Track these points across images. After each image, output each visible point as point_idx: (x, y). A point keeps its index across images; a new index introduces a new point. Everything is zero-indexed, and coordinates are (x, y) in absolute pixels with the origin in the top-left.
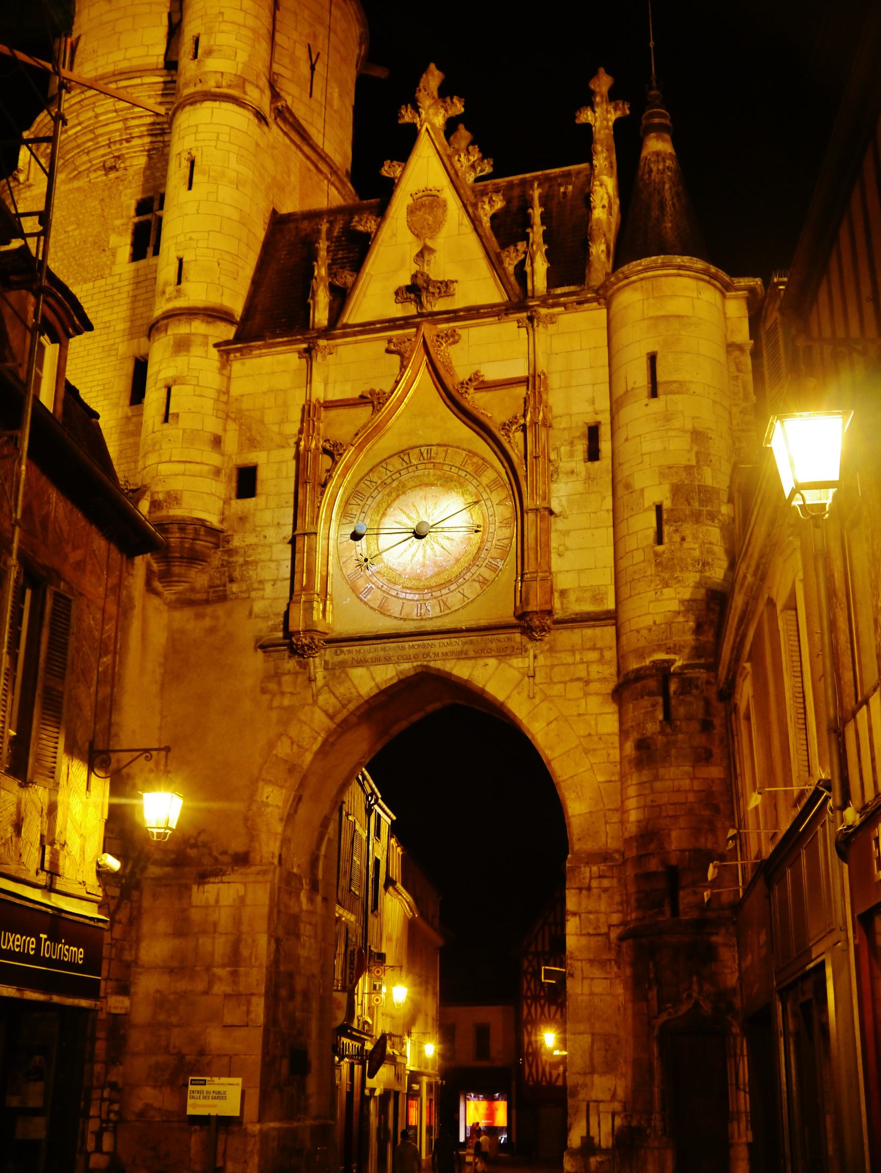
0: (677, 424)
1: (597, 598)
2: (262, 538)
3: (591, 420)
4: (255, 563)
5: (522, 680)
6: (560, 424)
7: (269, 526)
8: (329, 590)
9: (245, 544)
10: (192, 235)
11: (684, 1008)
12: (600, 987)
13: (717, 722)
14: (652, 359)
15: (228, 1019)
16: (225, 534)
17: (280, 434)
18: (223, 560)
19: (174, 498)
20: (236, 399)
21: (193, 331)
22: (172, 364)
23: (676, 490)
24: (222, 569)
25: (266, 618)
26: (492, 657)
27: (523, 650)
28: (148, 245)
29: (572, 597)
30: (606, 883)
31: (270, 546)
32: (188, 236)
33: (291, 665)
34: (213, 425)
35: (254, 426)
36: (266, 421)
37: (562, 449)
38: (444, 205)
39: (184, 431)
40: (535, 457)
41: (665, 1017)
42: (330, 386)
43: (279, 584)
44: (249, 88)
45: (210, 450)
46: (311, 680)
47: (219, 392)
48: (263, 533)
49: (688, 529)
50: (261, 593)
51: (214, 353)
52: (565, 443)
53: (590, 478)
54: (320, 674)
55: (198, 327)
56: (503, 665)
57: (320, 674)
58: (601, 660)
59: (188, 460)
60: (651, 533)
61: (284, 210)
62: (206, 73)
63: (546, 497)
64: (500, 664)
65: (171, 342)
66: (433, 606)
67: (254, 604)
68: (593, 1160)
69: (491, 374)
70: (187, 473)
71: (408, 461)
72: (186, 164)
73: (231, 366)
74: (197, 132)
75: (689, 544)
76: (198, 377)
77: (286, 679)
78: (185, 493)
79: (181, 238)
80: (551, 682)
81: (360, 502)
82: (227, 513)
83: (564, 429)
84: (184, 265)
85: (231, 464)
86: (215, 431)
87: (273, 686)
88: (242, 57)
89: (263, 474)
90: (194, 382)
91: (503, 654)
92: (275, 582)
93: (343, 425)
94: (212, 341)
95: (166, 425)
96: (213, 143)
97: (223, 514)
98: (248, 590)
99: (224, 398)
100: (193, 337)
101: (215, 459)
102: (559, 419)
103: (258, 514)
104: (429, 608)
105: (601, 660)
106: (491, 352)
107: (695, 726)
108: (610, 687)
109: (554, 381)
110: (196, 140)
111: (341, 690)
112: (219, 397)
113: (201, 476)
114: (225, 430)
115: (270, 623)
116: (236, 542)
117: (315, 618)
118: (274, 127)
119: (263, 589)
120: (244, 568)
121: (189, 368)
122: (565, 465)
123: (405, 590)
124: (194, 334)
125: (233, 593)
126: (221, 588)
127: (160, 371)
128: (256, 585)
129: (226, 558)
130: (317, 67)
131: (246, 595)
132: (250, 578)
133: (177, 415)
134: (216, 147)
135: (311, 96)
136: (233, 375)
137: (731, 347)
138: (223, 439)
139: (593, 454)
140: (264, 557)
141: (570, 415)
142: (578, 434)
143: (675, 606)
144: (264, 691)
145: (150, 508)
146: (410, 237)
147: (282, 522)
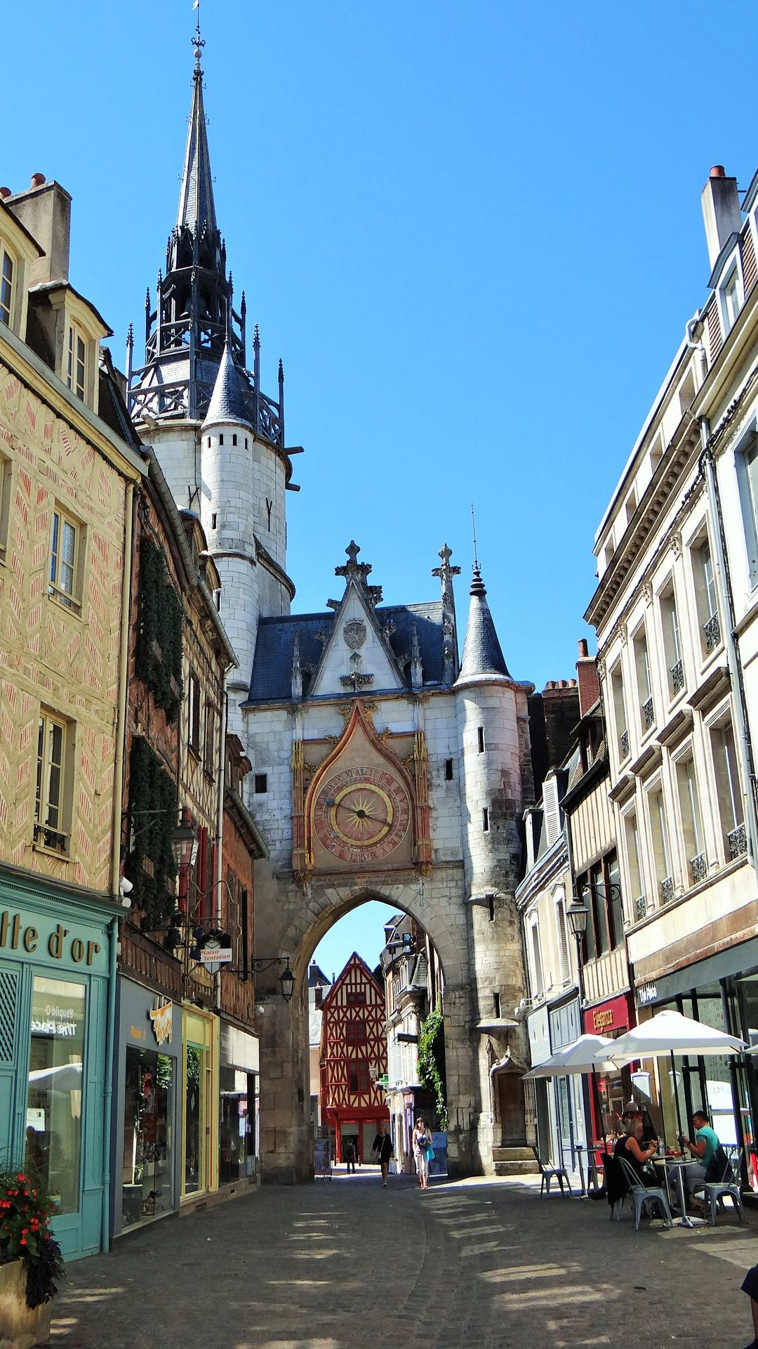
3: (448, 758)
11: (503, 1061)
14: (480, 730)
15: (272, 1075)
23: (495, 803)
25: (278, 861)
29: (441, 853)
30: (463, 1000)
33: (293, 887)
41: (495, 1066)
46: (304, 895)
53: (448, 789)
54: (309, 892)
57: (309, 892)
58: (457, 886)
60: (482, 824)
68: (461, 1137)
77: (291, 894)
87: (283, 898)
88: (242, 528)
89: (270, 780)
91: (406, 883)
93: (316, 753)
106: (394, 717)
107: (507, 924)
111: (321, 901)
116: (258, 818)
122: (436, 781)
137: (519, 719)
139: (449, 776)
144: (278, 901)
146: (346, 647)
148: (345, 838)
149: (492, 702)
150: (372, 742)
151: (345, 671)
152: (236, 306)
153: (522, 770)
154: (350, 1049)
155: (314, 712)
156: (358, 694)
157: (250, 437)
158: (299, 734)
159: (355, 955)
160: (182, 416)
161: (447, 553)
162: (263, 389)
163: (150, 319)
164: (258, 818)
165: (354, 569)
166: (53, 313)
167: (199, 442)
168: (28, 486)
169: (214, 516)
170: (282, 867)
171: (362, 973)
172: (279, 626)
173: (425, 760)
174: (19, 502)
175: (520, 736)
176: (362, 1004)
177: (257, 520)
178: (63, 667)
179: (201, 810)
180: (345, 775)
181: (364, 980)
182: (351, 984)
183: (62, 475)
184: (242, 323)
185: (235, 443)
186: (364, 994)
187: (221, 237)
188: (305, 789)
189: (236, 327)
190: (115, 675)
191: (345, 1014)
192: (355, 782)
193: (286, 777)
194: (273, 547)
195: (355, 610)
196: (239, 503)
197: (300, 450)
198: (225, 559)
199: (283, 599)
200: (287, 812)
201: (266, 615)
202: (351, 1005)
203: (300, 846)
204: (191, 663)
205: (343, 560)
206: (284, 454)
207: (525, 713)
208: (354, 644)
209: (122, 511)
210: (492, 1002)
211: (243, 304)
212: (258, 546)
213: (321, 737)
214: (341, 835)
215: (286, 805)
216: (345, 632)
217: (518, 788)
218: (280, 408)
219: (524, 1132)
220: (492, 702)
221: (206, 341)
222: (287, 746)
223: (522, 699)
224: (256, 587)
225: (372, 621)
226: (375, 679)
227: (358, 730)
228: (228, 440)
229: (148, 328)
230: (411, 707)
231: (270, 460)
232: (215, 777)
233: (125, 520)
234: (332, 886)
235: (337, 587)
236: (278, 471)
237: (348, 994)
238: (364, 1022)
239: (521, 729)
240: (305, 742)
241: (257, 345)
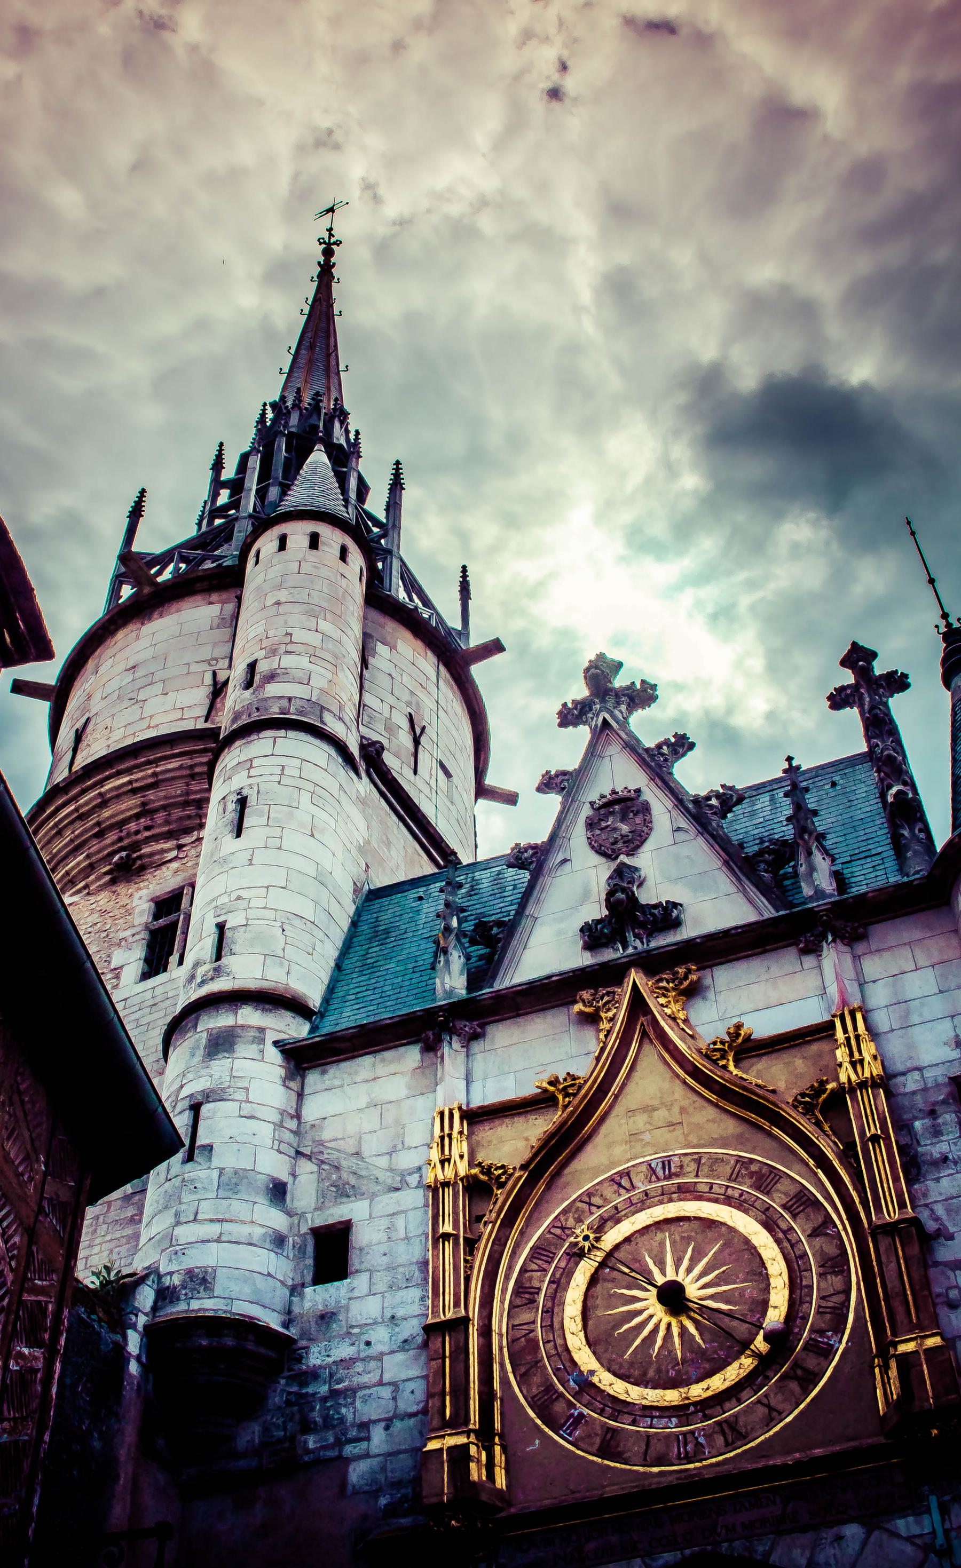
2: (362, 1346)
5: (924, 1562)
7: (375, 1323)
8: (497, 1426)
9: (330, 1360)
10: (241, 893)
16: (295, 1347)
17: (391, 1170)
18: (289, 1393)
19: (200, 1280)
20: (313, 1126)
21: (240, 1022)
22: (203, 1072)
24: (288, 1411)
25: (375, 1493)
26: (851, 1520)
28: (171, 953)
31: (379, 1358)
32: (234, 897)
34: (273, 1165)
35: (344, 1163)
36: (366, 1153)
37: (918, 1124)
38: (646, 809)
39: (221, 1171)
40: (875, 1139)
42: (476, 1087)
43: (398, 1425)
44: (327, 717)
45: (266, 1202)
47: (283, 1113)
48: (365, 1338)
50: (364, 1445)
51: (274, 1055)
52: (921, 1115)
55: (249, 1016)
56: (876, 1534)
59: (227, 1216)
61: (381, 880)
62: (266, 699)
64: (868, 1534)
65: (204, 1042)
66: (708, 1437)
67: (351, 1468)
69: (763, 1026)
70: (223, 1239)
71: (628, 1185)
72: (231, 806)
73: (303, 1078)
74: (251, 767)
76: (247, 1089)
78: (219, 1270)
79: (224, 900)
81: (545, 1266)
82: (296, 1310)
83: (914, 1093)
84: (228, 934)
85: (304, 1229)
86: (275, 1175)
90: (240, 1095)
92: (388, 1423)
94: (271, 1037)
95: (189, 1166)
96: (277, 778)
97: (289, 1312)
98: (340, 1443)
99: (293, 1124)
100: (239, 1031)
101: (276, 1219)
102: (900, 1079)
103: (355, 1307)
104: (702, 1440)
110: (249, 777)
112: (282, 1121)
113: (251, 1244)
114: (294, 1175)
115: (383, 1501)
116: (315, 1358)
117: (474, 1476)
118: (365, 778)
119: (368, 1439)
120: (328, 1404)
121: (232, 1076)
123: (648, 1413)
124: (242, 1026)
125: (308, 1451)
126: (287, 1445)
127: (182, 1087)
128: (353, 1433)
129: (294, 1389)
130: (423, 740)
131: (335, 1453)
132: (342, 1420)
133: (209, 1148)
134: (279, 782)
135: (415, 772)
136: (307, 1091)
138: (289, 1187)
140: (365, 1379)
141: (919, 1069)
142: (941, 1097)
145: (156, 1302)
146: (596, 859)
147: (400, 1313)
150: (695, 1073)
151: (596, 911)
155: (504, 1037)
164: (315, 1358)
180: (609, 1191)
188: (471, 1245)
192: (645, 1202)
196: (315, 639)
197: (495, 647)
203: (459, 1422)
213: (529, 1090)
230: (809, 961)
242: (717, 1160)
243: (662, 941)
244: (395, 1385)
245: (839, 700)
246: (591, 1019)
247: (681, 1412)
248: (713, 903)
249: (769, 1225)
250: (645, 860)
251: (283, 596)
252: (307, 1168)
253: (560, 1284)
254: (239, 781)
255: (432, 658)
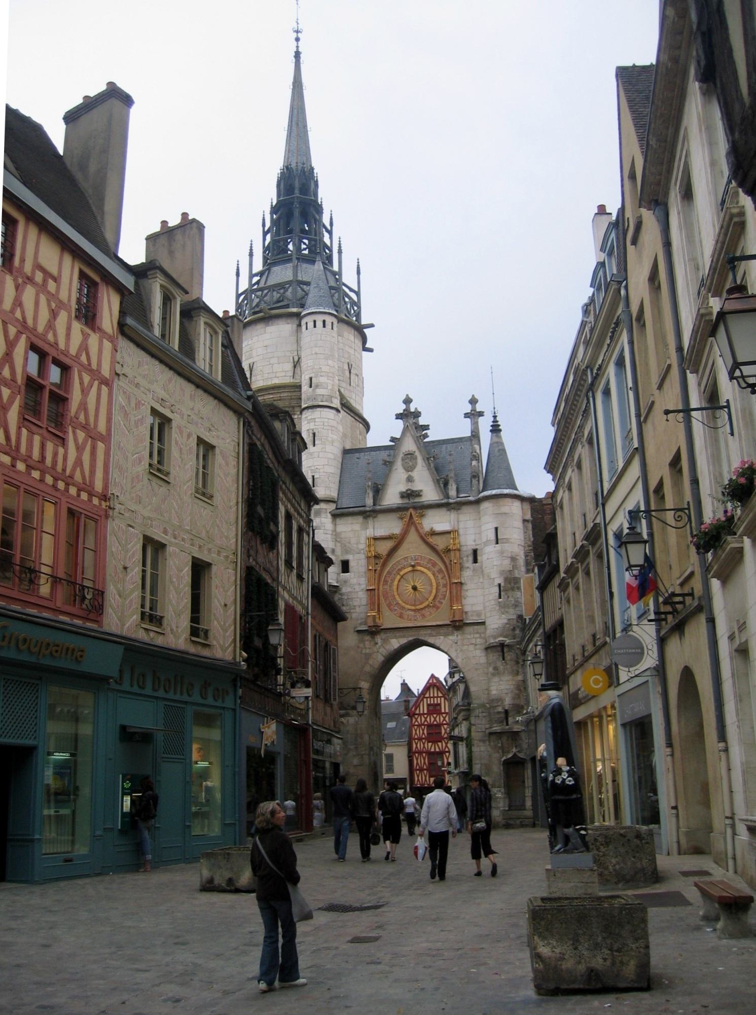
0: (505, 555)
1: (479, 615)
3: (474, 547)
4: (352, 599)
6: (464, 549)
11: (510, 756)
12: (482, 749)
13: (520, 661)
14: (496, 529)
23: (506, 579)
25: (357, 620)
27: (452, 634)
29: (470, 614)
33: (368, 638)
38: (416, 458)
41: (504, 758)
49: (510, 593)
51: (329, 516)
53: (474, 570)
60: (497, 594)
63: (459, 577)
72: (311, 435)
75: (511, 599)
77: (367, 643)
80: (463, 645)
87: (361, 645)
89: (351, 564)
91: (446, 635)
105: (480, 637)
108: (484, 647)
109: (461, 532)
122: (467, 565)
137: (525, 521)
139: (475, 561)
143: (506, 621)
146: (403, 471)
148: (403, 604)
149: (505, 509)
151: (403, 488)
152: (326, 220)
153: (526, 556)
154: (430, 744)
155: (381, 517)
156: (412, 506)
157: (335, 321)
158: (370, 532)
159: (433, 676)
160: (287, 306)
161: (473, 401)
162: (345, 280)
163: (265, 234)
165: (409, 416)
166: (194, 323)
167: (299, 325)
168: (181, 432)
169: (311, 379)
170: (361, 624)
171: (438, 689)
172: (357, 455)
173: (459, 550)
174: (177, 443)
175: (525, 532)
176: (439, 713)
177: (341, 378)
178: (204, 535)
179: (295, 598)
181: (440, 695)
182: (430, 697)
183: (200, 421)
184: (330, 232)
185: (324, 326)
186: (440, 705)
187: (315, 171)
189: (326, 235)
190: (234, 533)
191: (426, 719)
193: (363, 562)
194: (354, 396)
195: (409, 445)
197: (372, 326)
198: (319, 409)
199: (360, 434)
200: (363, 587)
201: (348, 447)
202: (430, 713)
204: (286, 507)
205: (401, 408)
206: (360, 330)
207: (528, 516)
208: (409, 469)
209: (236, 431)
210: (503, 715)
211: (331, 219)
212: (342, 397)
214: (400, 602)
215: (363, 581)
216: (403, 460)
217: (523, 569)
218: (358, 294)
219: (524, 801)
220: (505, 509)
221: (305, 249)
222: (363, 540)
223: (527, 506)
224: (340, 428)
225: (420, 451)
226: (423, 493)
227: (413, 529)
228: (319, 324)
229: (264, 239)
231: (350, 335)
232: (305, 576)
233: (239, 439)
234: (396, 637)
235: (397, 428)
236: (357, 341)
237: (428, 705)
238: (439, 726)
239: (525, 527)
240: (375, 539)
241: (340, 252)
242: (425, 558)
243: (417, 500)
244: (361, 599)
245: (467, 415)
246: (402, 519)
247: (414, 610)
248: (430, 494)
249: (434, 575)
250: (415, 474)
251: (317, 350)
252: (338, 544)
253: (393, 580)
254: (312, 426)
255: (353, 331)
